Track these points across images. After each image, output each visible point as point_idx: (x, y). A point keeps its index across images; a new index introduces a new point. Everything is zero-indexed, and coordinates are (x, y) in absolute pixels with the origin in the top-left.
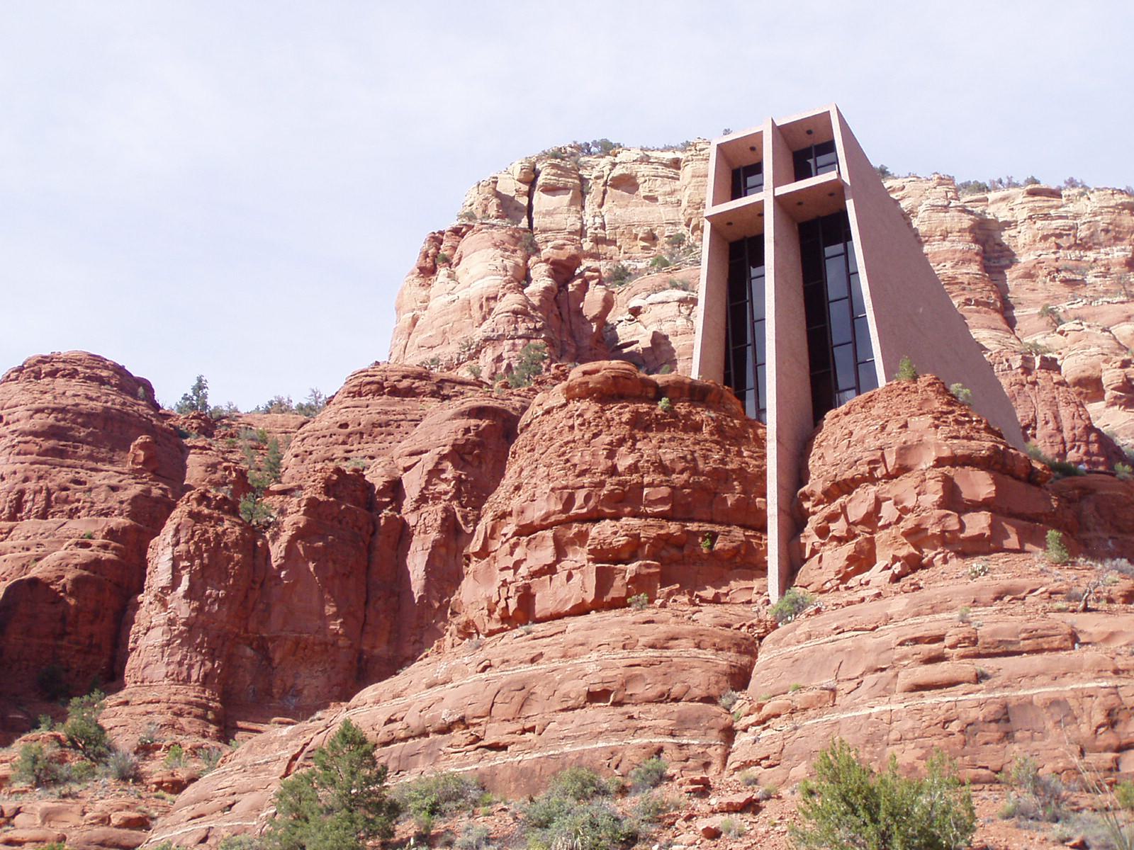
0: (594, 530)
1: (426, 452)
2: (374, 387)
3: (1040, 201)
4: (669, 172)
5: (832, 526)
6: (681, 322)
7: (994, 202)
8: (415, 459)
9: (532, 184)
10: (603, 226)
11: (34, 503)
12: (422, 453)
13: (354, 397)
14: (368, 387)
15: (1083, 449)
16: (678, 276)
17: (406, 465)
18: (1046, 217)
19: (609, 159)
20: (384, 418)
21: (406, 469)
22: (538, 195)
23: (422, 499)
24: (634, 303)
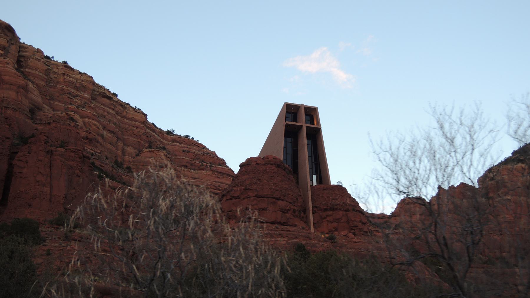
0: (280, 202)
5: (328, 218)
18: (68, 75)
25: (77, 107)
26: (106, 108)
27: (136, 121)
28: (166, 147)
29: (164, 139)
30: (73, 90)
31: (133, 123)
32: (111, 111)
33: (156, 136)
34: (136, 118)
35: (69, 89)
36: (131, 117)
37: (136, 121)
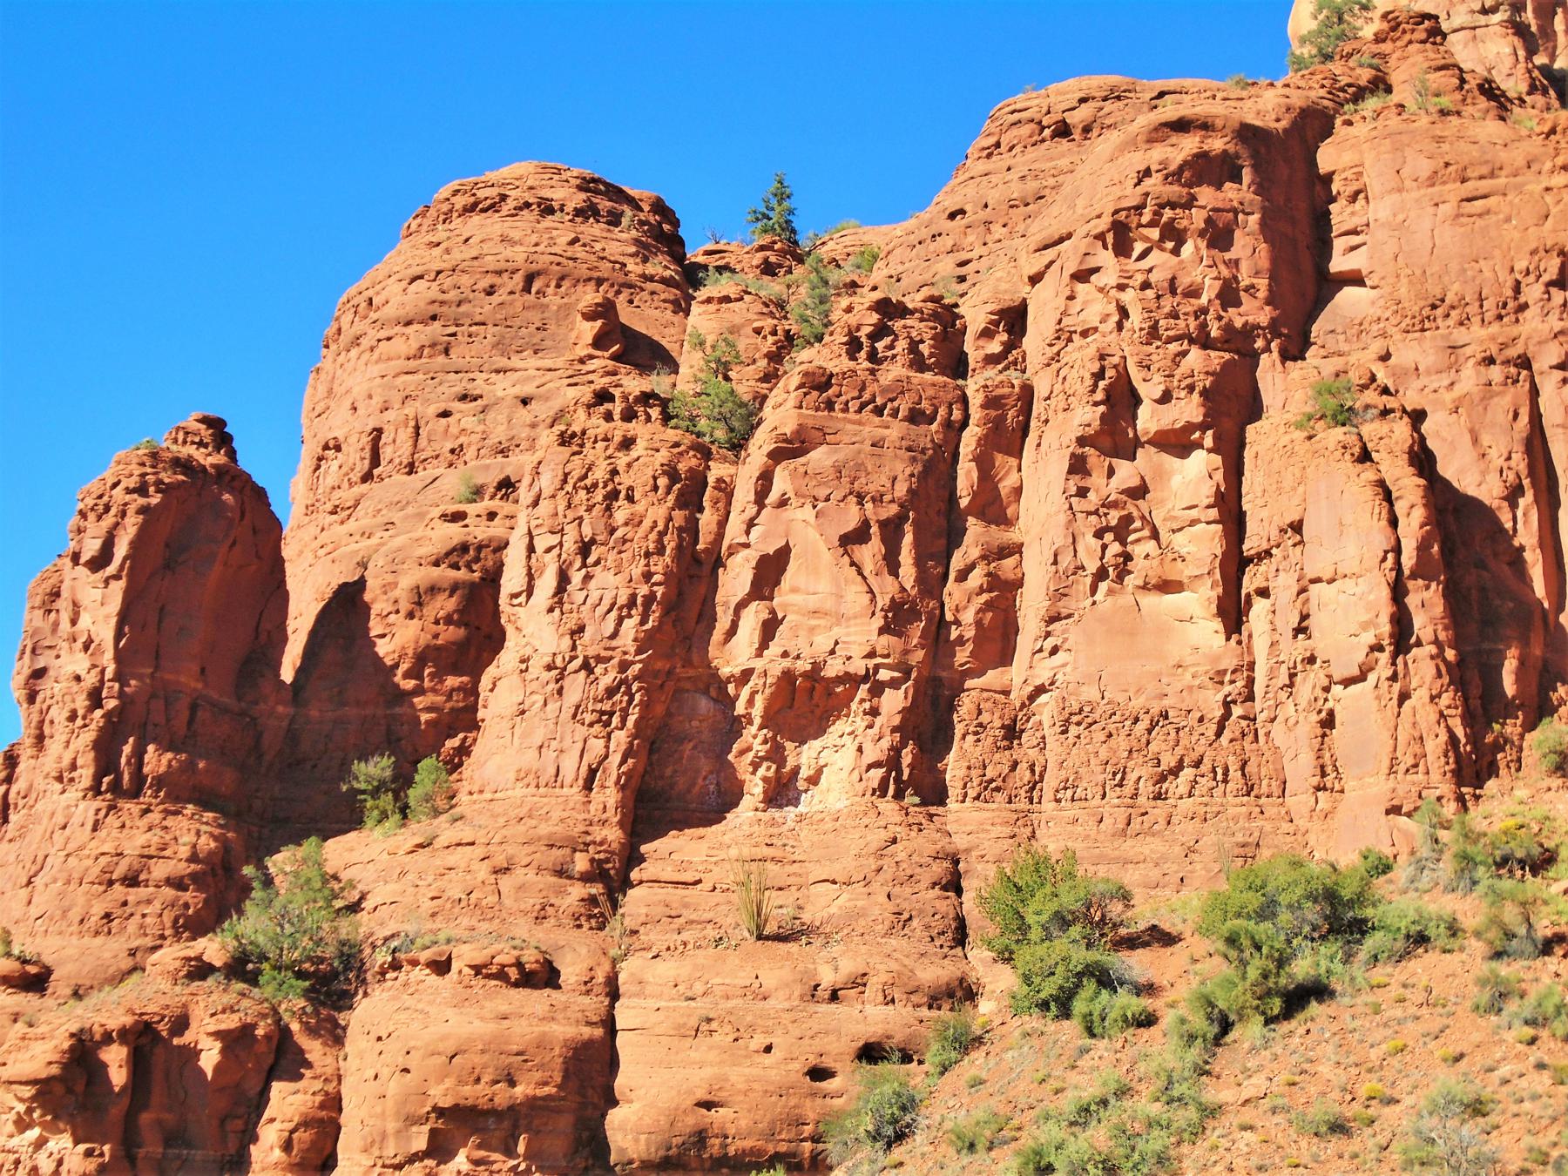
1: (1069, 236)
2: (1026, 130)
8: (1050, 254)
11: (395, 449)
12: (1061, 240)
13: (989, 156)
14: (1015, 131)
17: (1033, 271)
20: (1032, 186)
21: (1035, 280)
23: (1064, 336)
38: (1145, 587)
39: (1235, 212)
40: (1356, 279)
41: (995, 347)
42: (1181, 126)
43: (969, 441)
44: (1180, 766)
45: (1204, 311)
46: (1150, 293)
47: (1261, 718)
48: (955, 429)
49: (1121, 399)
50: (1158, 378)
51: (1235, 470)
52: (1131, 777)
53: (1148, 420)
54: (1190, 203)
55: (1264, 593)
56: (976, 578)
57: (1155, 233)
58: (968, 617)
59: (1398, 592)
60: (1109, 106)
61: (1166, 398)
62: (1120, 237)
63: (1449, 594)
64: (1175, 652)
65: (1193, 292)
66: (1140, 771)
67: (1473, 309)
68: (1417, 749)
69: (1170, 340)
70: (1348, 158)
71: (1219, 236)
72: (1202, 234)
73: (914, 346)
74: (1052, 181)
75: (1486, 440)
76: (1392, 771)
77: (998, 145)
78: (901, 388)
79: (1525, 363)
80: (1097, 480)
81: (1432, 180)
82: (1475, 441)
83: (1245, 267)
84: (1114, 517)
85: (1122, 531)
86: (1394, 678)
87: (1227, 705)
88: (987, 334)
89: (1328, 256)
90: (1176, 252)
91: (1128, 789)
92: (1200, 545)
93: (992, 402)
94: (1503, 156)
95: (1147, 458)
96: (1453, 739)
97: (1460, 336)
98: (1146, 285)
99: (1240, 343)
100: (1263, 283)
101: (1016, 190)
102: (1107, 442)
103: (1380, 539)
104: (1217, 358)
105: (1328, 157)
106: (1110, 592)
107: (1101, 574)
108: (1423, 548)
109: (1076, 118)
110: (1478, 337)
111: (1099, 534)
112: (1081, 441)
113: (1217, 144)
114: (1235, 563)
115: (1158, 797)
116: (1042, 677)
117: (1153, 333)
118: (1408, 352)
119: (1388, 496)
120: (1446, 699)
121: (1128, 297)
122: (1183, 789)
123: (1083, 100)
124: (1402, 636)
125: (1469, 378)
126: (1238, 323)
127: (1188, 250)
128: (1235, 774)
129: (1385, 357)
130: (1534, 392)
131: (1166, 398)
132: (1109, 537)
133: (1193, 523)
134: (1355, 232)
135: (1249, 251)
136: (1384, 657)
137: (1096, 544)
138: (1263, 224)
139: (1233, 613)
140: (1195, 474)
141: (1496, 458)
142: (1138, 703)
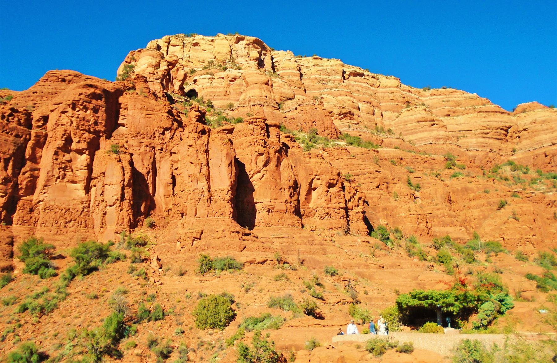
2: (55, 78)
3: (317, 61)
4: (211, 43)
6: (209, 85)
7: (304, 60)
8: (56, 106)
9: (169, 43)
10: (189, 57)
12: (59, 104)
14: (52, 78)
15: (330, 130)
16: (209, 71)
17: (52, 109)
18: (318, 65)
19: (193, 38)
20: (54, 90)
21: (52, 111)
22: (170, 47)
23: (57, 124)
24: (195, 78)
25: (331, 89)
26: (359, 83)
27: (390, 87)
28: (425, 103)
29: (421, 96)
30: (325, 77)
31: (388, 89)
32: (364, 85)
33: (413, 95)
34: (389, 84)
35: (322, 76)
36: (385, 85)
37: (390, 87)
38: (68, 182)
39: (100, 106)
40: (123, 125)
41: (40, 124)
42: (91, 86)
43: (30, 144)
44: (71, 221)
45: (90, 125)
46: (78, 119)
47: (91, 212)
48: (27, 141)
49: (68, 141)
50: (78, 138)
51: (92, 160)
52: (59, 222)
53: (74, 146)
54: (90, 102)
55: (95, 186)
56: (28, 174)
57: (82, 107)
58: (24, 183)
59: (123, 189)
60: (75, 78)
61: (79, 142)
62: (74, 106)
63: (133, 191)
64: (73, 196)
65: (89, 121)
66: (62, 221)
67: (145, 136)
68: (122, 220)
69: (82, 130)
70: (125, 101)
71: (96, 110)
72: (92, 109)
73: (19, 120)
74: (59, 91)
75: (144, 161)
76: (117, 225)
77: (47, 80)
78: (14, 129)
79: (154, 148)
80: (60, 157)
81: (141, 109)
82: (142, 161)
83: (100, 118)
84: (63, 166)
85: (65, 169)
86: (120, 206)
87: (83, 209)
88: (38, 121)
89: (118, 118)
90: (86, 112)
91: (58, 225)
92: (82, 174)
93: (37, 136)
94: (155, 107)
95: (72, 154)
96: (130, 219)
97: (142, 140)
98: (78, 117)
99: (97, 134)
100: (104, 122)
101: (50, 91)
102: (64, 149)
103: (121, 178)
104: (92, 136)
105: (121, 100)
106: (60, 182)
107: (58, 178)
108: (129, 181)
109: (67, 78)
110: (146, 141)
111: (59, 169)
112: (58, 148)
113: (98, 92)
114: (89, 179)
115: (65, 227)
116: (41, 198)
117: (78, 128)
118: (132, 142)
119: (123, 170)
120: (130, 211)
121: (73, 119)
122: (71, 225)
123: (69, 75)
124: (122, 198)
125: (143, 149)
126: (97, 129)
127: (88, 112)
128: (83, 223)
129: (127, 142)
130: (155, 154)
131: (79, 142)
132: (61, 170)
133: (81, 169)
134: (124, 116)
135: (102, 115)
136: (118, 202)
137: (58, 171)
138: (105, 110)
139: (87, 189)
140: (83, 159)
141: (146, 165)
142: (63, 206)
